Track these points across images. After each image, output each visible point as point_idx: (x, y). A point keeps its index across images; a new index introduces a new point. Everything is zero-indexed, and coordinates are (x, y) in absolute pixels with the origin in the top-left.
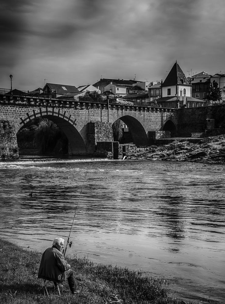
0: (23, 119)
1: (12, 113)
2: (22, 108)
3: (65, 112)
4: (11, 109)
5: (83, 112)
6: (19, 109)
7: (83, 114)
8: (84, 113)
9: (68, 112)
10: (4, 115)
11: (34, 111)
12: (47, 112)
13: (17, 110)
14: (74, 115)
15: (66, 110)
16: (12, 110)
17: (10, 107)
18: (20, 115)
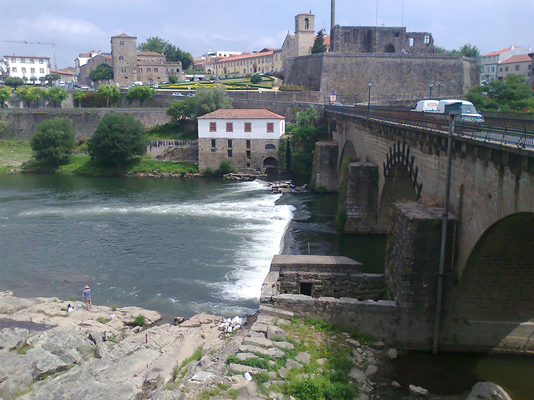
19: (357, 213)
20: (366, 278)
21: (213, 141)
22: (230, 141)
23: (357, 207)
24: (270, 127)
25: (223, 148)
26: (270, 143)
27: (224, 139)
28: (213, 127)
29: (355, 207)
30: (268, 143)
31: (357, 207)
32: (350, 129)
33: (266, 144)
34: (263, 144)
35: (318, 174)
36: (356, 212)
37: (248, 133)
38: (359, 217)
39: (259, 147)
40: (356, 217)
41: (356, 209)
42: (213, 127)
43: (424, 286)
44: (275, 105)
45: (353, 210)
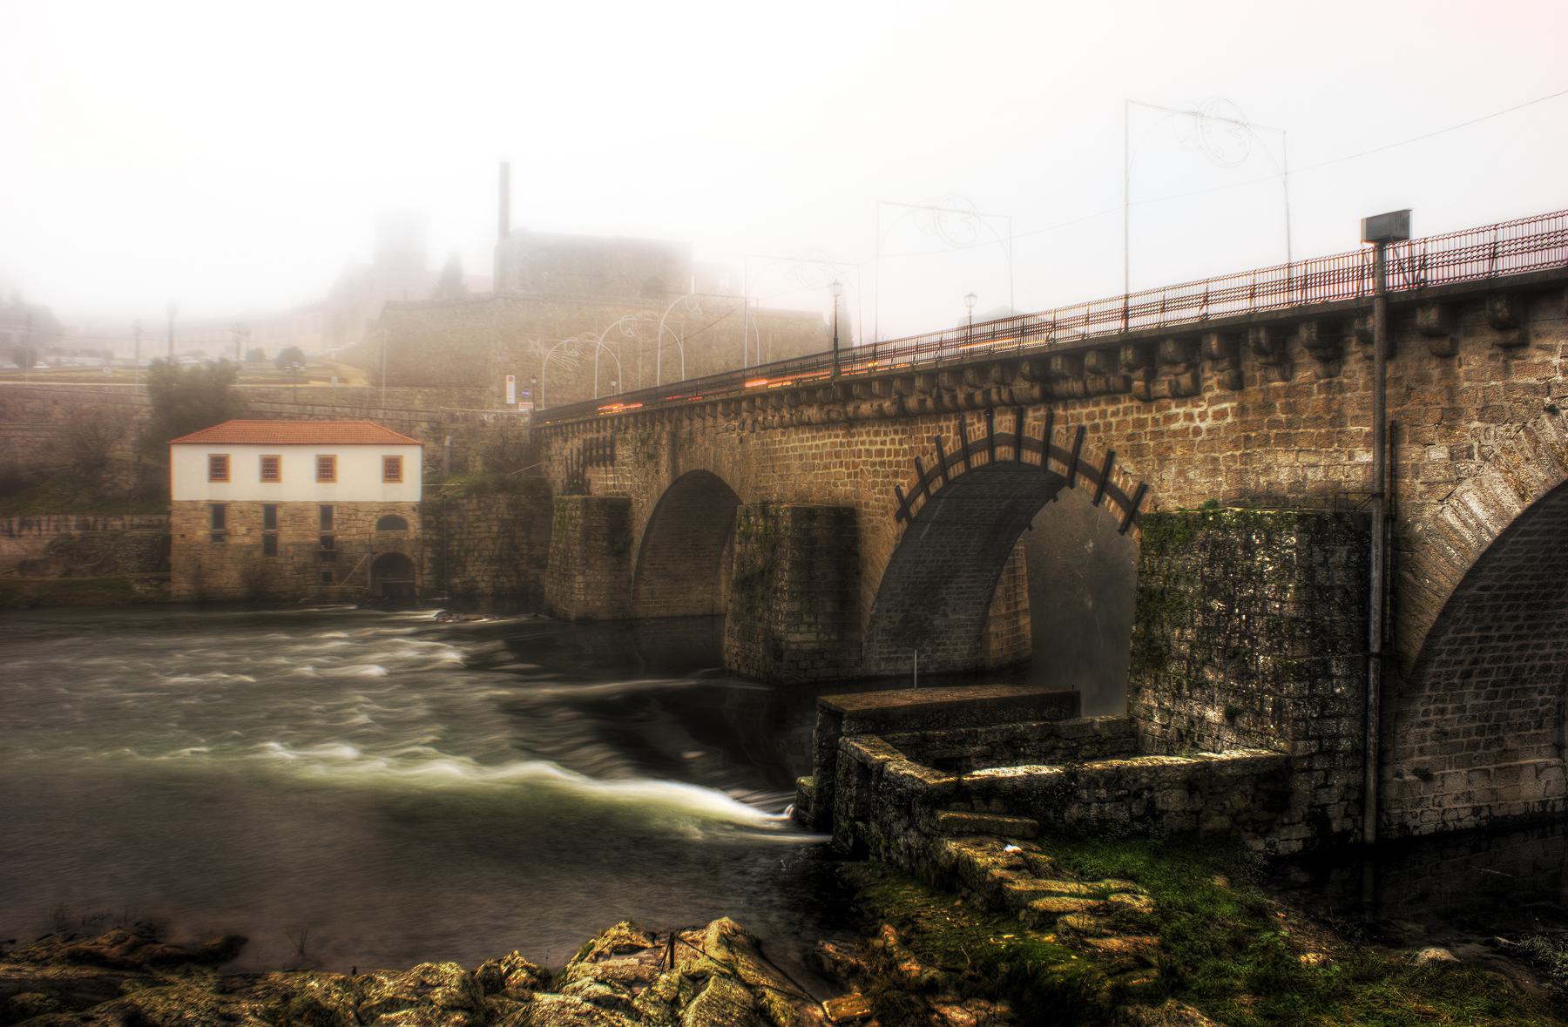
0: (905, 491)
1: (874, 464)
2: (904, 432)
3: (1081, 431)
4: (871, 443)
5: (1197, 422)
6: (893, 442)
7: (1197, 431)
8: (1203, 426)
9: (1096, 428)
10: (849, 476)
11: (938, 440)
12: (991, 442)
13: (888, 446)
14: (1137, 452)
15: (1090, 416)
16: (873, 448)
17: (868, 433)
18: (896, 475)
19: (812, 637)
20: (1097, 727)
21: (219, 512)
22: (270, 510)
23: (812, 619)
24: (392, 470)
25: (249, 530)
26: (392, 513)
27: (253, 503)
28: (219, 469)
29: (806, 619)
30: (387, 513)
31: (812, 619)
32: (699, 439)
33: (380, 515)
34: (369, 518)
35: (579, 578)
36: (809, 631)
37: (329, 486)
38: (816, 646)
39: (360, 524)
40: (805, 646)
41: (810, 625)
42: (219, 469)
43: (1338, 690)
44: (381, 416)
45: (803, 628)
